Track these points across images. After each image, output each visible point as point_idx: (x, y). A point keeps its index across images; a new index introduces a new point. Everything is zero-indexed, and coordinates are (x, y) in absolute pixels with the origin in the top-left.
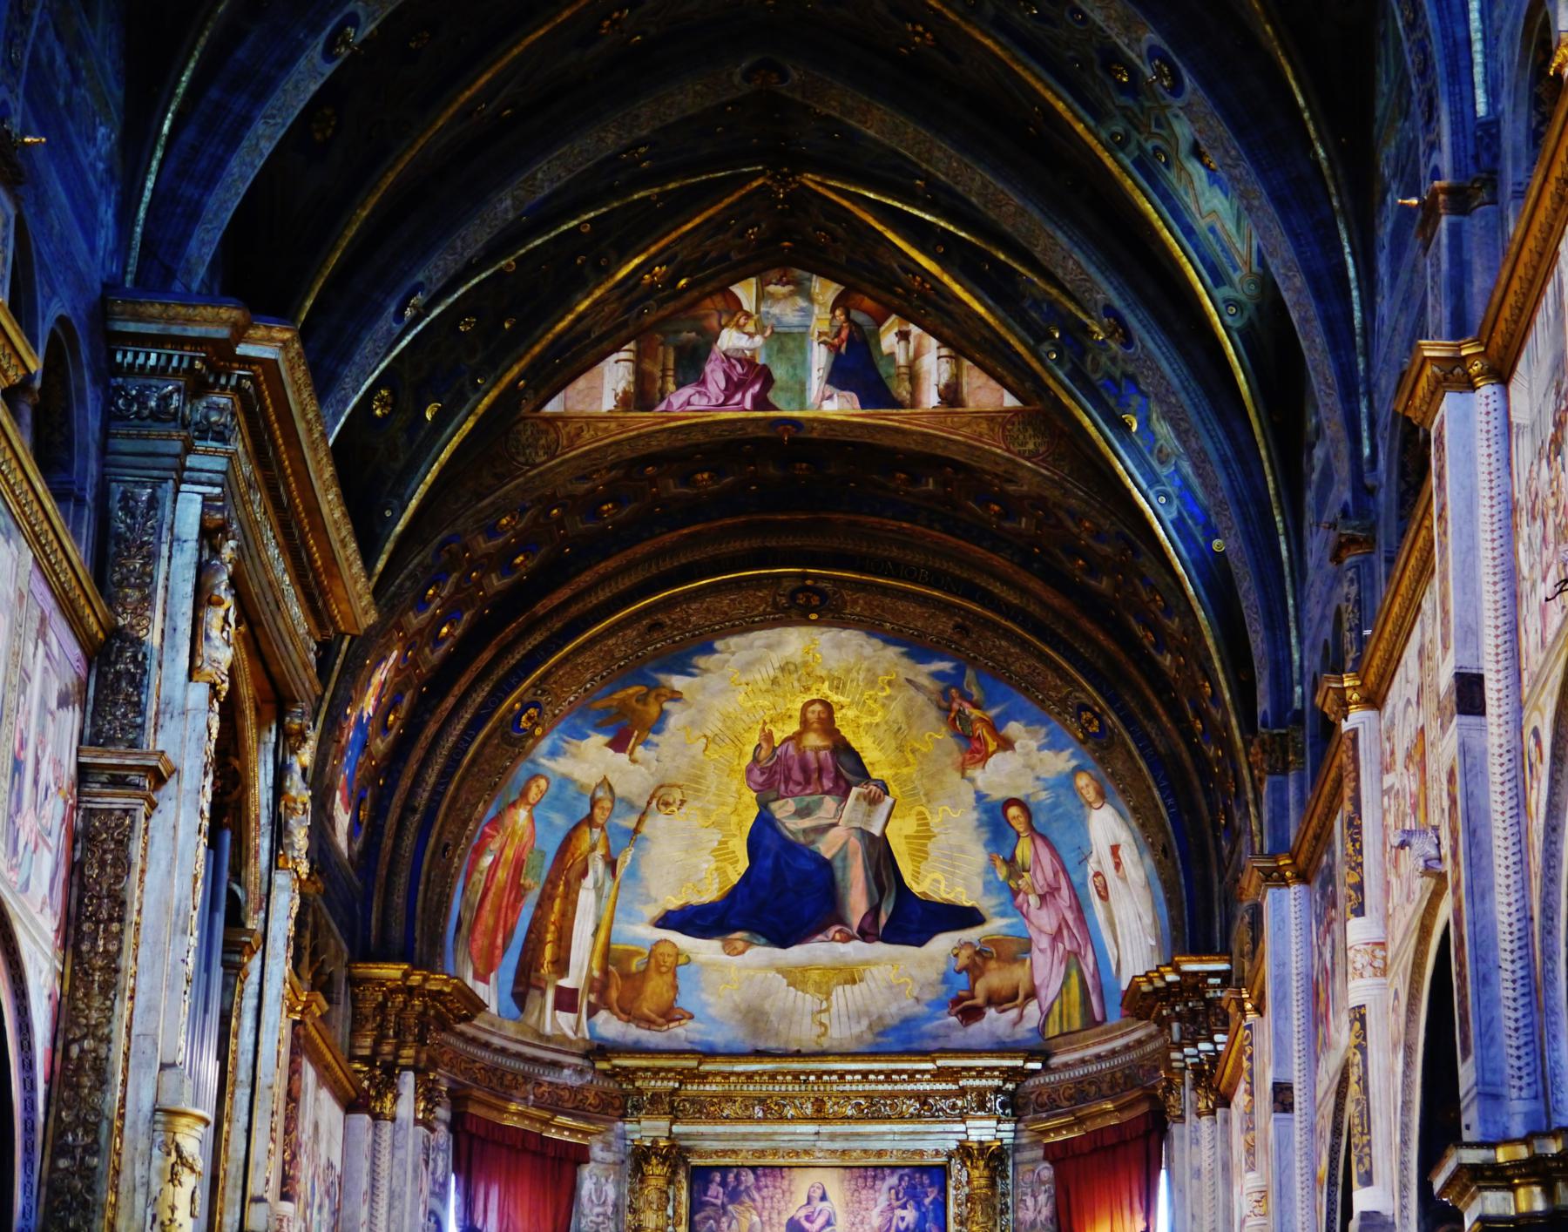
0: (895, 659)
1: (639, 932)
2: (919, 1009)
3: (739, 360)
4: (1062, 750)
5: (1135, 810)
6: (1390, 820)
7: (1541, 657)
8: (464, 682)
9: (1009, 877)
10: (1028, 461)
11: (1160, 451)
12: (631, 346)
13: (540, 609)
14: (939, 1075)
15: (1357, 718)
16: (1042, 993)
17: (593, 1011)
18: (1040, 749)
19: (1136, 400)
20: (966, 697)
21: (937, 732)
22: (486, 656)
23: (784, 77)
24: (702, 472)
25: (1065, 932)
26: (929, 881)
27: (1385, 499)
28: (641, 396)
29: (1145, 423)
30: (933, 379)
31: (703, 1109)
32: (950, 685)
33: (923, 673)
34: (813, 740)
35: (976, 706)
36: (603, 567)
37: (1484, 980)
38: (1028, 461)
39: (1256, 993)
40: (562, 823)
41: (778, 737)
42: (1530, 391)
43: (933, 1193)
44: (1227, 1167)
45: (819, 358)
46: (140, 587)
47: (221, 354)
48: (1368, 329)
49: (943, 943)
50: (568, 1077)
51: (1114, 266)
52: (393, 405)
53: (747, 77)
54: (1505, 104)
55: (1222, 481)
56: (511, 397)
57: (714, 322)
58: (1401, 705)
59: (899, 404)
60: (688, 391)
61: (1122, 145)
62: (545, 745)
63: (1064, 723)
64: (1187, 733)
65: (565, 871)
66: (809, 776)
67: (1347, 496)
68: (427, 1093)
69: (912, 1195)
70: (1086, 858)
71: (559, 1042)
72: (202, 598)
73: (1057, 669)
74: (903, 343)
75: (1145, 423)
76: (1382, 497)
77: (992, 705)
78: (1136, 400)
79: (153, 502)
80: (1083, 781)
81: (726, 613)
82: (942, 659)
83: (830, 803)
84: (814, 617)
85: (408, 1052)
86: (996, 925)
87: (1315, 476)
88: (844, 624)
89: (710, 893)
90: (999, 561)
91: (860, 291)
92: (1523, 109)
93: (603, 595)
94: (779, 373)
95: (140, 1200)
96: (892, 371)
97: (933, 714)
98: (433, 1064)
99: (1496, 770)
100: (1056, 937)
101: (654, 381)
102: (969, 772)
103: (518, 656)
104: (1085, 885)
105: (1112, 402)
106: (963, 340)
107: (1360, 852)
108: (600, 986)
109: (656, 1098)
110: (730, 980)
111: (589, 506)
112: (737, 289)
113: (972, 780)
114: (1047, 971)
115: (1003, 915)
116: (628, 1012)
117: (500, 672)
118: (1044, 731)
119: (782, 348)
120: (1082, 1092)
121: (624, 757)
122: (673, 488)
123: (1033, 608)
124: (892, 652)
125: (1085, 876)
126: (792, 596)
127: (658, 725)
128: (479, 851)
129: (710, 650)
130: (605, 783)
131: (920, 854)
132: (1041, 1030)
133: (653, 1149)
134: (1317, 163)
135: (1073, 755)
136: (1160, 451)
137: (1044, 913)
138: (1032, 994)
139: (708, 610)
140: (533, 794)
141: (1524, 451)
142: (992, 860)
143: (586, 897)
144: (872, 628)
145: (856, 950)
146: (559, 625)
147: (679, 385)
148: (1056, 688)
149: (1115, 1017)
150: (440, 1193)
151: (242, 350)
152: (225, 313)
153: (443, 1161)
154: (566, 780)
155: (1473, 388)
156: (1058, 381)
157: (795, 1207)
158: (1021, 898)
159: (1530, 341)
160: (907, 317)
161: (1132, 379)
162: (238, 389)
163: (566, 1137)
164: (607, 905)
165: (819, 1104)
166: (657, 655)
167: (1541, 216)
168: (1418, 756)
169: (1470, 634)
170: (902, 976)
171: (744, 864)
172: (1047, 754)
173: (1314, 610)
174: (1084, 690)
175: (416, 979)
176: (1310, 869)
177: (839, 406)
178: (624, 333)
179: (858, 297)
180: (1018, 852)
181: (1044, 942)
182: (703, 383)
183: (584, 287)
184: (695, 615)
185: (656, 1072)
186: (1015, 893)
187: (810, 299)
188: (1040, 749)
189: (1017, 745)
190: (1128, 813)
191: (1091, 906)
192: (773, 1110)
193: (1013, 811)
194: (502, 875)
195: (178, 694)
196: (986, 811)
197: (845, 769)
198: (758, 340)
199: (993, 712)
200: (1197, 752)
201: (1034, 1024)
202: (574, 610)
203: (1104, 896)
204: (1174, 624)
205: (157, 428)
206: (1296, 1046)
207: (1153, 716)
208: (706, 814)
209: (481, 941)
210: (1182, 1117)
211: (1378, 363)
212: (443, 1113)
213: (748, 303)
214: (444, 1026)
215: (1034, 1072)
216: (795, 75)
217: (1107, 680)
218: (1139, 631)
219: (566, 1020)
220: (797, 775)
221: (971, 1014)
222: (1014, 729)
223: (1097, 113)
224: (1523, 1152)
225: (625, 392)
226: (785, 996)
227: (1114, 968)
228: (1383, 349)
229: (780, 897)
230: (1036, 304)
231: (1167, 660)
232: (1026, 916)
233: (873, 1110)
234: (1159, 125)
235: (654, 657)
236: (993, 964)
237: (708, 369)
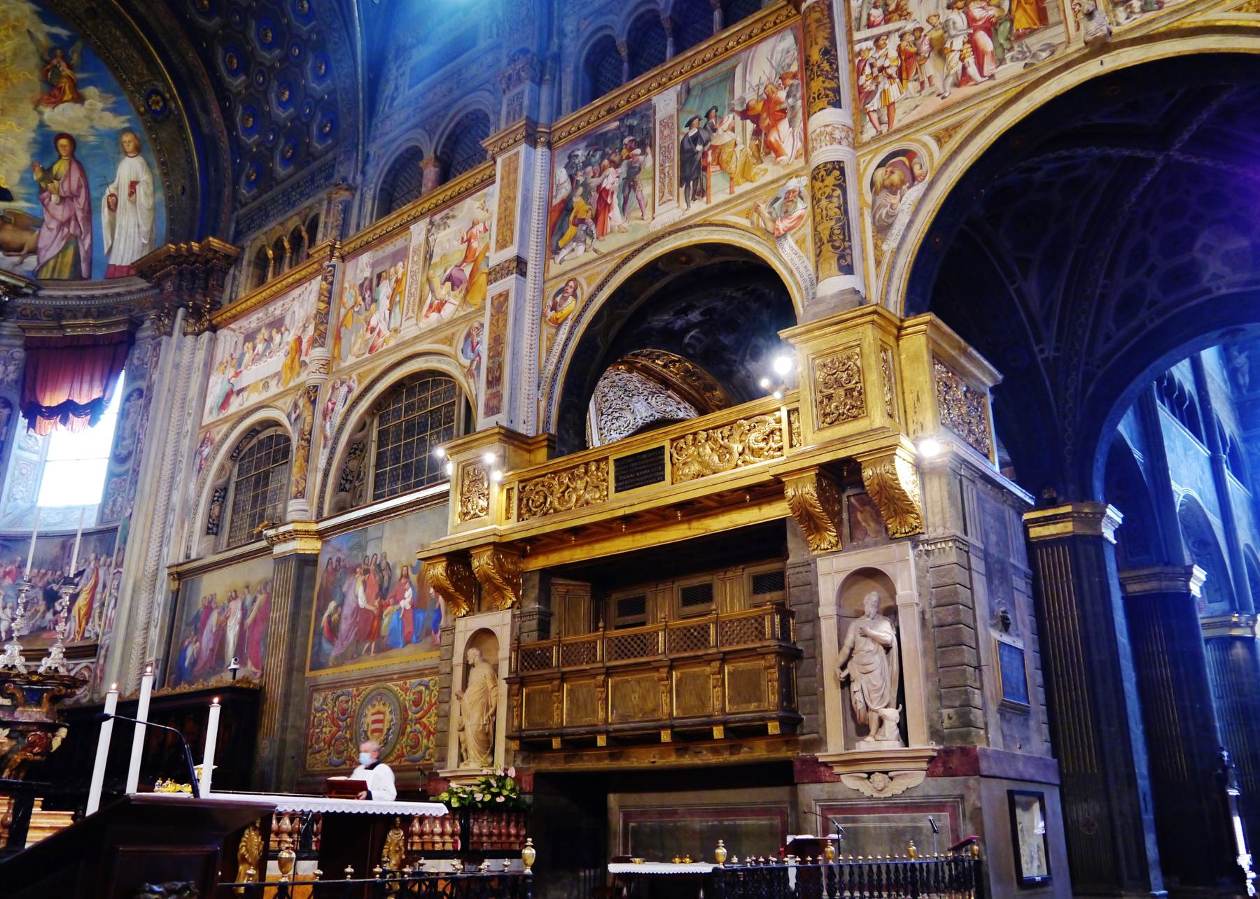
4: (121, 115)
5: (163, 164)
9: (42, 179)
16: (43, 253)
18: (104, 110)
21: (31, 73)
25: (73, 223)
32: (59, 47)
33: (43, 31)
35: (70, 67)
39: (347, 249)
63: (132, 100)
70: (107, 185)
73: (150, 61)
77: (83, 70)
82: (63, 27)
86: (20, 205)
97: (34, 61)
100: (64, 224)
102: (41, 108)
104: (100, 199)
107: (837, 70)
113: (41, 113)
114: (49, 242)
115: (27, 200)
118: (114, 99)
125: (103, 194)
132: (36, 273)
135: (129, 121)
137: (60, 208)
138: (34, 251)
142: (33, 167)
149: (98, 277)
158: (45, 194)
172: (108, 115)
174: (164, 80)
180: (56, 167)
181: (54, 225)
186: (42, 190)
188: (104, 110)
189: (87, 103)
190: (155, 164)
191: (100, 212)
193: (63, 142)
196: (42, 135)
199: (80, 76)
201: (30, 268)
203: (113, 208)
207: (206, 111)
210: (170, 334)
215: (27, 295)
222: (91, 91)
227: (106, 250)
232: (45, 206)
236: (9, 227)
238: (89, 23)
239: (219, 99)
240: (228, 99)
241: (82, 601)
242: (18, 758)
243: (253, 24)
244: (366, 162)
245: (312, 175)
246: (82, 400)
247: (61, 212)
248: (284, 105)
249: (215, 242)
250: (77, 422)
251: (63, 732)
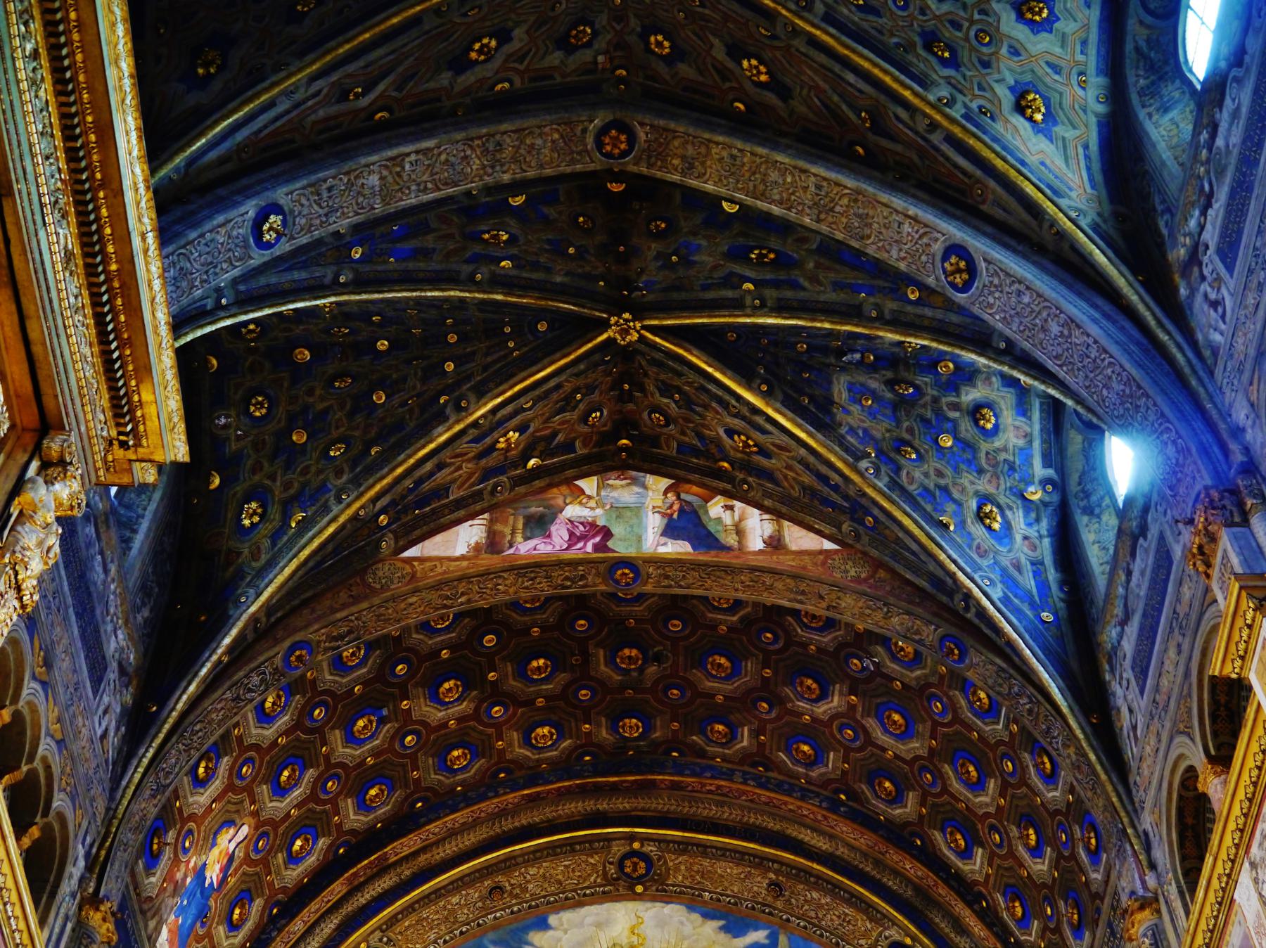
0: (713, 935)
3: (582, 523)
11: (978, 547)
12: (486, 516)
24: (542, 725)
29: (962, 525)
30: (759, 532)
45: (653, 523)
52: (262, 516)
74: (728, 512)
78: (950, 507)
81: (559, 882)
82: (756, 929)
84: (639, 889)
88: (663, 894)
90: (807, 809)
91: (689, 482)
93: (448, 850)
94: (617, 530)
96: (720, 528)
101: (504, 536)
103: (368, 896)
105: (929, 508)
117: (349, 908)
123: (842, 851)
126: (621, 866)
129: (543, 925)
136: (978, 547)
139: (544, 876)
144: (693, 900)
146: (408, 873)
147: (526, 539)
148: (866, 934)
161: (945, 490)
174: (894, 923)
178: (478, 507)
179: (687, 486)
182: (549, 536)
187: (645, 487)
198: (599, 511)
202: (423, 859)
225: (477, 543)
234: (981, 88)
235: (494, 928)
237: (553, 528)
238: (779, 904)
239: (969, 904)
240: (981, 896)
243: (947, 769)
244: (1148, 847)
245: (1110, 925)
248: (1036, 852)
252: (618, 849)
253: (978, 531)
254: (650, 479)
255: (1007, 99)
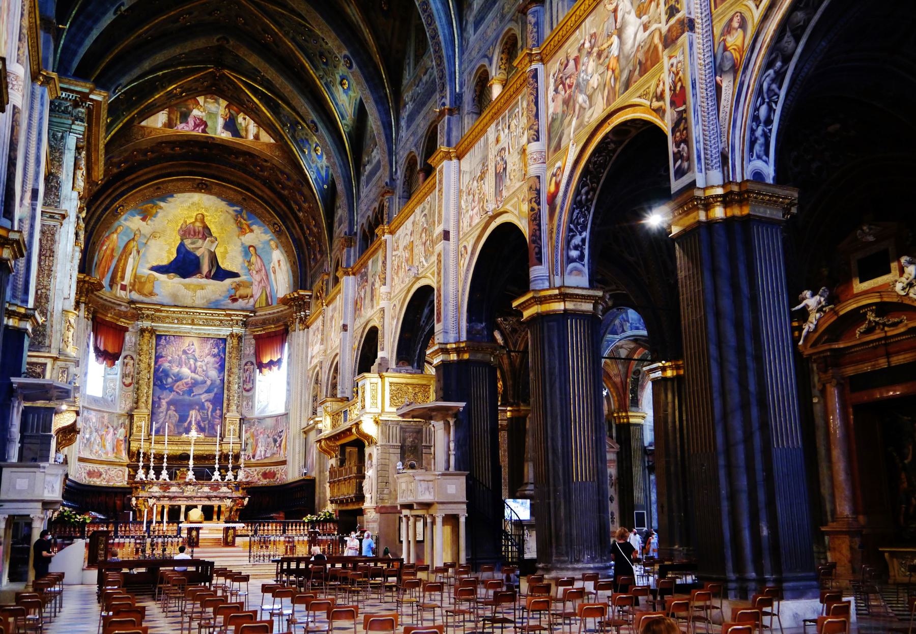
1: (145, 271)
2: (221, 298)
6: (395, 263)
7: (469, 229)
8: (103, 197)
10: (276, 157)
13: (127, 179)
14: (227, 315)
15: (387, 236)
17: (130, 291)
19: (307, 146)
20: (242, 217)
22: (110, 191)
23: (228, 42)
26: (225, 265)
27: (400, 182)
28: (170, 124)
29: (309, 152)
31: (160, 319)
33: (231, 210)
34: (198, 224)
36: (146, 170)
37: (446, 305)
38: (276, 157)
40: (126, 239)
41: (188, 222)
42: (467, 163)
43: (222, 345)
44: (307, 343)
45: (221, 122)
46: (59, 162)
47: (85, 97)
48: (396, 139)
49: (228, 281)
50: (123, 308)
51: (315, 109)
53: (218, 40)
54: (465, 89)
55: (339, 171)
56: (132, 119)
57: (191, 107)
58: (403, 235)
59: (242, 137)
60: (183, 125)
61: (322, 78)
62: (123, 217)
64: (304, 233)
65: (126, 252)
66: (196, 233)
67: (387, 180)
68: (88, 310)
69: (217, 345)
71: (121, 299)
72: (76, 166)
73: (270, 213)
75: (309, 152)
76: (398, 182)
77: (250, 219)
78: (307, 146)
79: (62, 137)
80: (272, 243)
83: (200, 241)
85: (83, 299)
86: (243, 278)
87: (366, 173)
89: (165, 262)
90: (257, 183)
92: (472, 92)
94: (209, 123)
95: (59, 335)
97: (232, 221)
98: (89, 302)
99: (452, 255)
100: (260, 282)
106: (261, 122)
108: (133, 285)
109: (148, 316)
110: (169, 285)
111: (145, 152)
112: (198, 98)
116: (140, 292)
117: (114, 195)
119: (210, 117)
120: (264, 323)
121: (144, 223)
122: (168, 151)
123: (265, 196)
124: (223, 203)
126: (198, 185)
127: (155, 215)
128: (103, 245)
129: (172, 196)
130: (139, 230)
131: (224, 257)
132: (254, 306)
133: (147, 329)
134: (386, 94)
138: (252, 296)
140: (119, 231)
141: (466, 178)
143: (131, 260)
144: (219, 196)
145: (204, 281)
149: (275, 304)
150: (89, 338)
151: (91, 96)
152: (88, 85)
153: (90, 328)
154: (128, 227)
155: (451, 159)
156: (288, 138)
157: (185, 347)
159: (472, 150)
160: (246, 114)
161: (307, 140)
162: (88, 108)
163: (123, 324)
164: (136, 263)
165: (193, 321)
166: (158, 196)
167: (485, 121)
168: (410, 247)
169: (447, 221)
170: (217, 289)
171: (175, 255)
172: (263, 235)
173: (363, 207)
175: (87, 279)
176: (360, 272)
177: (226, 135)
181: (256, 283)
183: (158, 91)
184: (170, 187)
185: (148, 309)
192: (180, 321)
194: (108, 252)
195: (69, 194)
197: (206, 232)
200: (306, 238)
203: (274, 272)
204: (306, 205)
205: (64, 115)
206: (350, 315)
207: (295, 228)
208: (166, 241)
209: (101, 269)
211: (399, 147)
212: (90, 316)
213: (201, 103)
214: (92, 293)
216: (231, 43)
217: (284, 218)
218: (294, 206)
219: (123, 293)
220: (192, 233)
221: (234, 300)
222: (254, 227)
223: (316, 68)
224: (454, 346)
226: (183, 291)
228: (402, 144)
229: (184, 265)
230: (284, 116)
231: (301, 214)
233: (207, 323)
241: (283, 443)
242: (235, 508)
246: (275, 359)
247: (257, 278)
249: (302, 292)
250: (275, 368)
251: (247, 499)
252: (198, 182)
253: (313, 154)
254: (221, 101)
255: (338, 79)
